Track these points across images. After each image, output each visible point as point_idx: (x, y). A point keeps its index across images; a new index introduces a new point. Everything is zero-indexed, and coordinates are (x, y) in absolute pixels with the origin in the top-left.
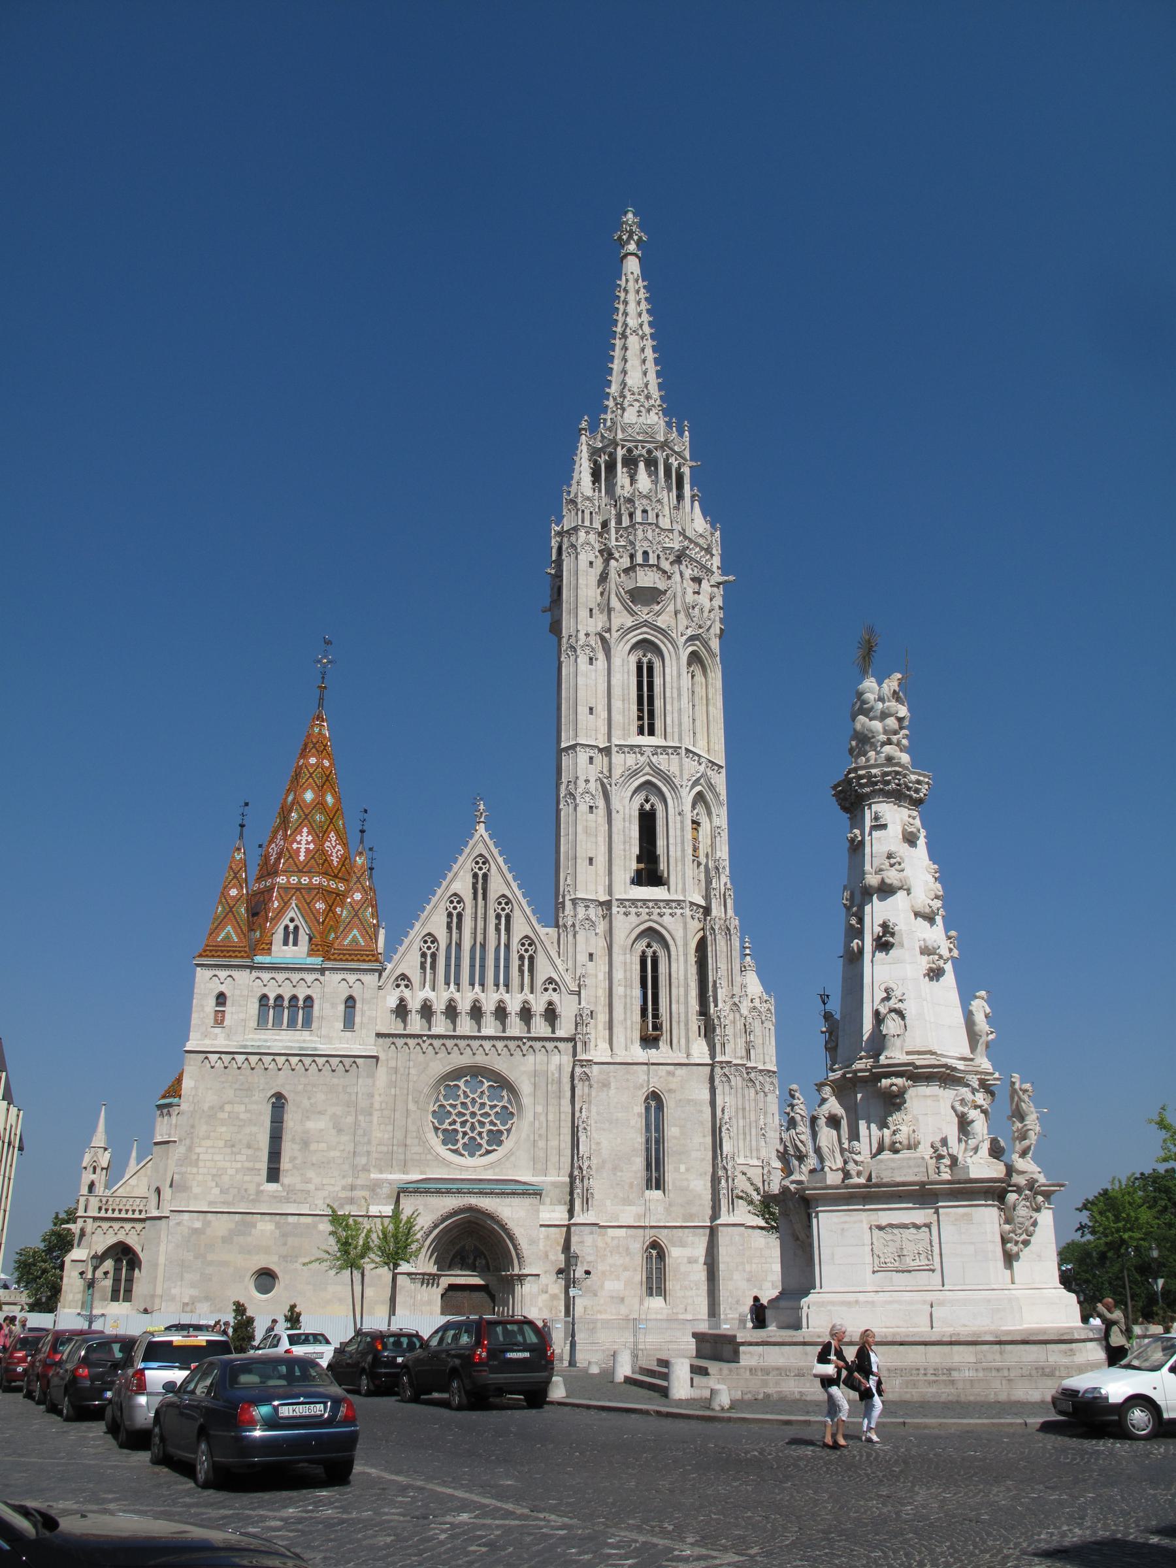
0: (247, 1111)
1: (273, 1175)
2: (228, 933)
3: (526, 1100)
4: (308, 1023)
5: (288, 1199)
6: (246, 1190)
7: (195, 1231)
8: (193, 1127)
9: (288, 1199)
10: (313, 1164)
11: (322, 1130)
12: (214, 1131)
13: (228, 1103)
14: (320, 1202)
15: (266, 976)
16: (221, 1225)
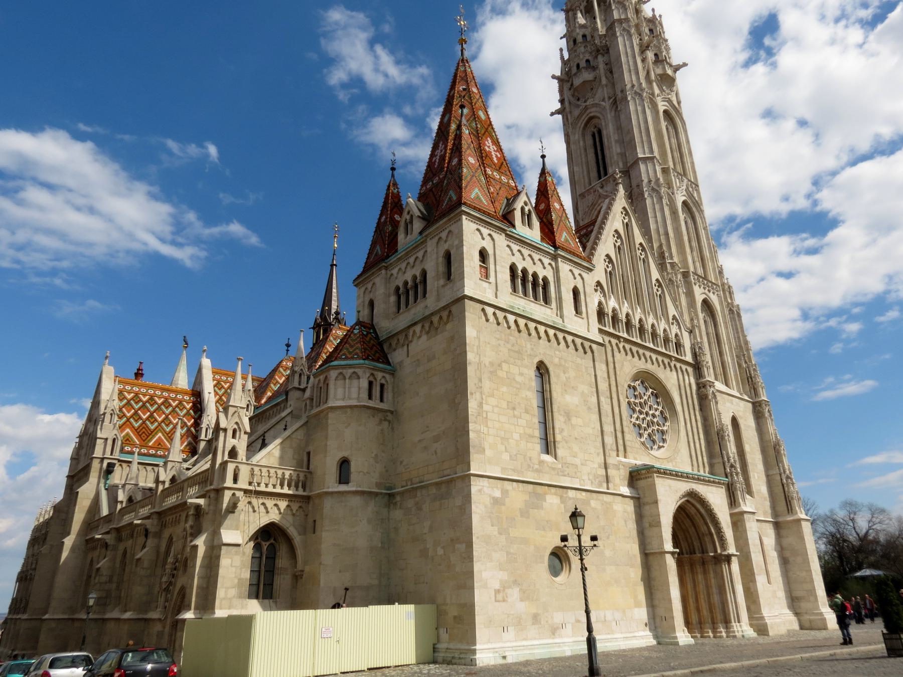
0: (521, 374)
1: (548, 445)
2: (477, 193)
3: (679, 408)
4: (547, 300)
5: (563, 472)
6: (530, 459)
7: (496, 501)
8: (480, 380)
9: (563, 472)
10: (576, 439)
11: (577, 406)
12: (497, 390)
13: (505, 361)
14: (585, 477)
15: (515, 247)
16: (518, 496)
